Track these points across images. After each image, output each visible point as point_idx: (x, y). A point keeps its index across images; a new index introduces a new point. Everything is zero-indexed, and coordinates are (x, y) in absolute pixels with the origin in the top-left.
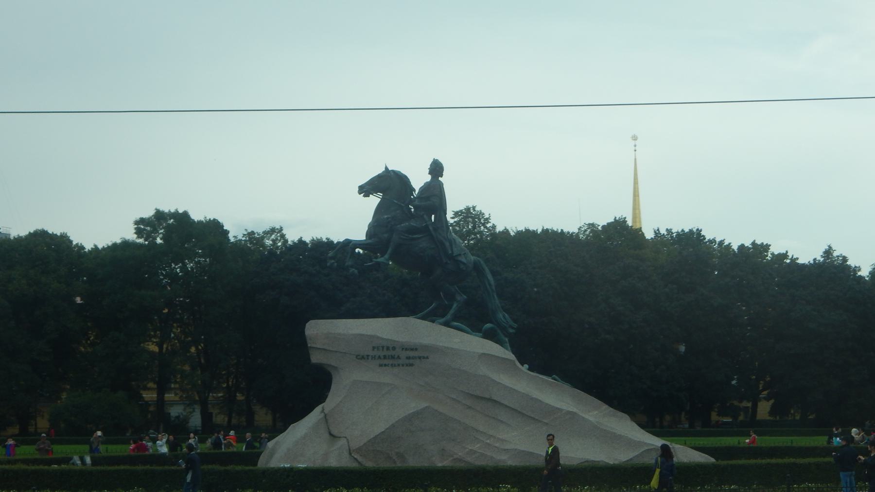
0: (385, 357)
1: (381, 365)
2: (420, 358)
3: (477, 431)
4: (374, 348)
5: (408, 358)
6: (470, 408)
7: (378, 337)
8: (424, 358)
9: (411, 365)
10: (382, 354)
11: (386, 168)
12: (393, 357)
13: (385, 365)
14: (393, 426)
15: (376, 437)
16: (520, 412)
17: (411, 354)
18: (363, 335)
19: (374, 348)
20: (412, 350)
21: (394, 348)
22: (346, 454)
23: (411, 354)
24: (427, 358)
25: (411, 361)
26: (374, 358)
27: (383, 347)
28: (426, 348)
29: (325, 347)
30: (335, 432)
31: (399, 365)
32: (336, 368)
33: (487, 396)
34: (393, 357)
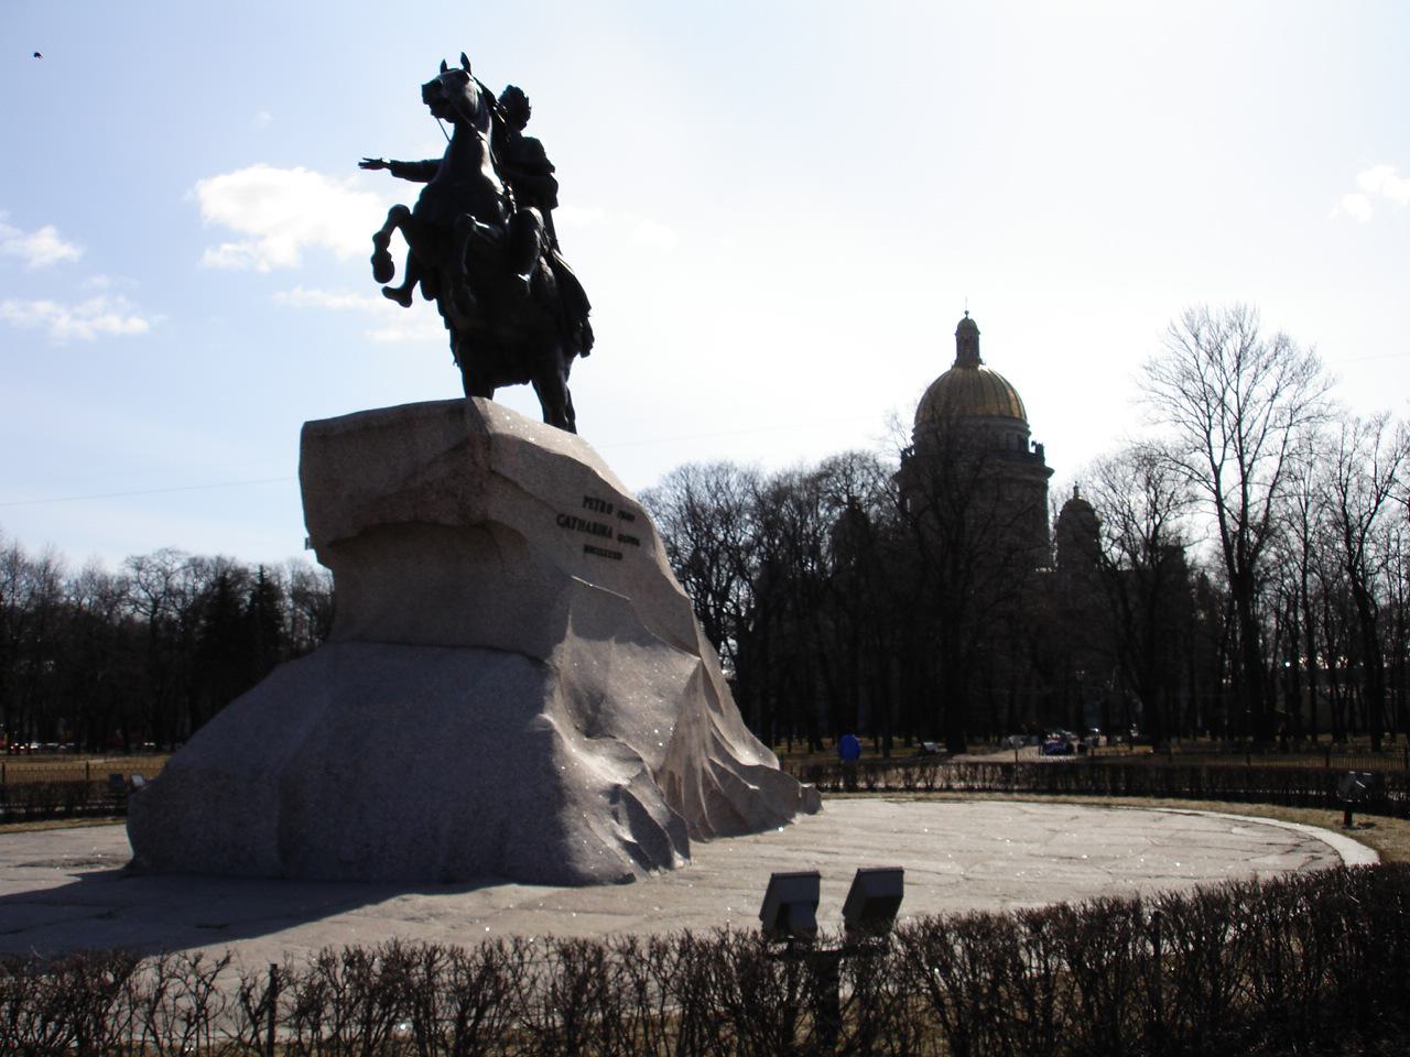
0: (595, 524)
1: (588, 549)
3: (714, 725)
4: (587, 500)
5: (621, 538)
9: (618, 556)
11: (465, 60)
12: (603, 531)
17: (627, 529)
19: (587, 500)
21: (610, 509)
26: (584, 526)
27: (598, 501)
29: (518, 478)
31: (605, 555)
32: (517, 538)
34: (603, 531)
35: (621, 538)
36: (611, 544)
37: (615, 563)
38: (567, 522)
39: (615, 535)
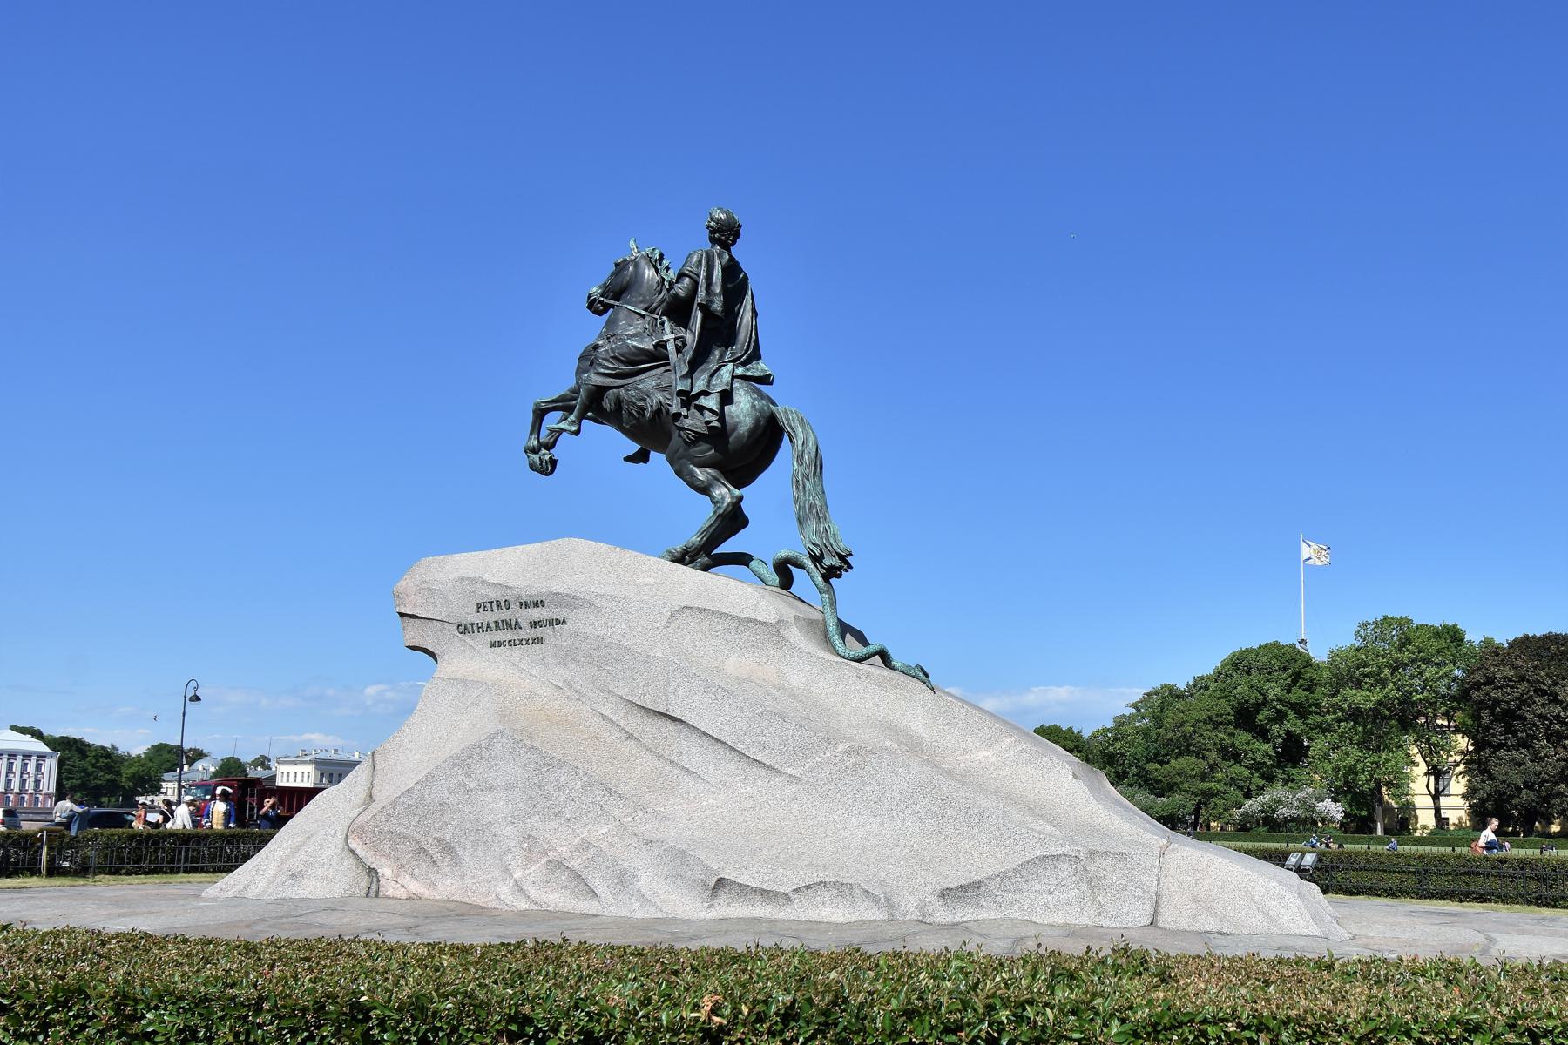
1: (493, 645)
2: (551, 623)
5: (534, 625)
6: (630, 736)
7: (484, 582)
8: (559, 622)
9: (540, 640)
10: (490, 617)
13: (500, 644)
14: (431, 777)
15: (394, 804)
16: (732, 748)
17: (536, 614)
18: (462, 579)
20: (536, 604)
21: (507, 604)
22: (340, 837)
23: (536, 614)
24: (564, 622)
25: (539, 632)
28: (560, 599)
30: (374, 792)
33: (661, 709)
34: (509, 625)
35: (534, 625)
36: (526, 633)
37: (537, 647)
38: (465, 629)
39: (525, 624)
